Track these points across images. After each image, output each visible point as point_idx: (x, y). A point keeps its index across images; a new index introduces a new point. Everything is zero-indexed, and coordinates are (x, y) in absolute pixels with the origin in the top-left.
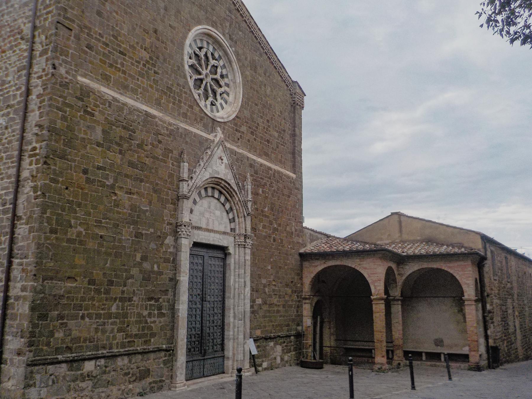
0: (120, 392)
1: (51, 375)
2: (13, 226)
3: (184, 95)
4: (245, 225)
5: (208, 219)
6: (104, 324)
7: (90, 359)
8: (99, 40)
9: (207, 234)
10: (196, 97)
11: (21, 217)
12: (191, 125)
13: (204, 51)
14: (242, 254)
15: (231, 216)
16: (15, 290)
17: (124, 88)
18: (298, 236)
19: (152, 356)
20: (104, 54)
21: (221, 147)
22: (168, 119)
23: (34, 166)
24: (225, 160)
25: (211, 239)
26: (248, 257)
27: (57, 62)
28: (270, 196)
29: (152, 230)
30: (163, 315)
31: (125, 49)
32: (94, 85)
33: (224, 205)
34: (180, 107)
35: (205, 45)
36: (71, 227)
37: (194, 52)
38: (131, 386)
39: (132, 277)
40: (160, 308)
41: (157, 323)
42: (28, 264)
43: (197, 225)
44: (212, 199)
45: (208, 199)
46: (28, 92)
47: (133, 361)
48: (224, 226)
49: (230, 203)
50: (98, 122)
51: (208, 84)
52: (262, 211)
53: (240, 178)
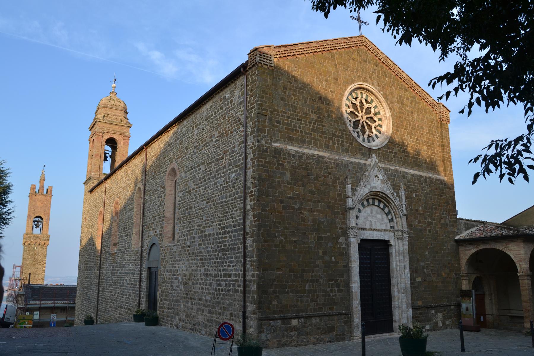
0: (315, 340)
1: (272, 326)
2: (245, 239)
3: (345, 136)
4: (402, 223)
5: (371, 222)
6: (301, 297)
7: (295, 318)
8: (284, 116)
9: (371, 232)
10: (355, 135)
11: (248, 233)
12: (353, 156)
13: (359, 99)
14: (401, 245)
15: (390, 217)
16: (249, 277)
17: (301, 142)
18: (453, 226)
19: (336, 318)
20: (288, 123)
21: (376, 168)
22: (335, 156)
23: (252, 203)
24: (381, 177)
25: (375, 236)
26: (406, 247)
27: (259, 138)
28: (423, 198)
29: (329, 234)
30: (342, 291)
31: (300, 116)
32: (283, 146)
33: (383, 210)
34: (343, 145)
35: (359, 94)
36: (276, 237)
37: (352, 102)
38: (322, 336)
39: (317, 266)
40: (338, 286)
42: (254, 261)
43: (363, 227)
44: (373, 206)
45: (370, 207)
46: (246, 157)
47: (323, 320)
48: (384, 225)
49: (388, 207)
50: (286, 169)
51: (364, 123)
52: (417, 210)
53: (396, 188)
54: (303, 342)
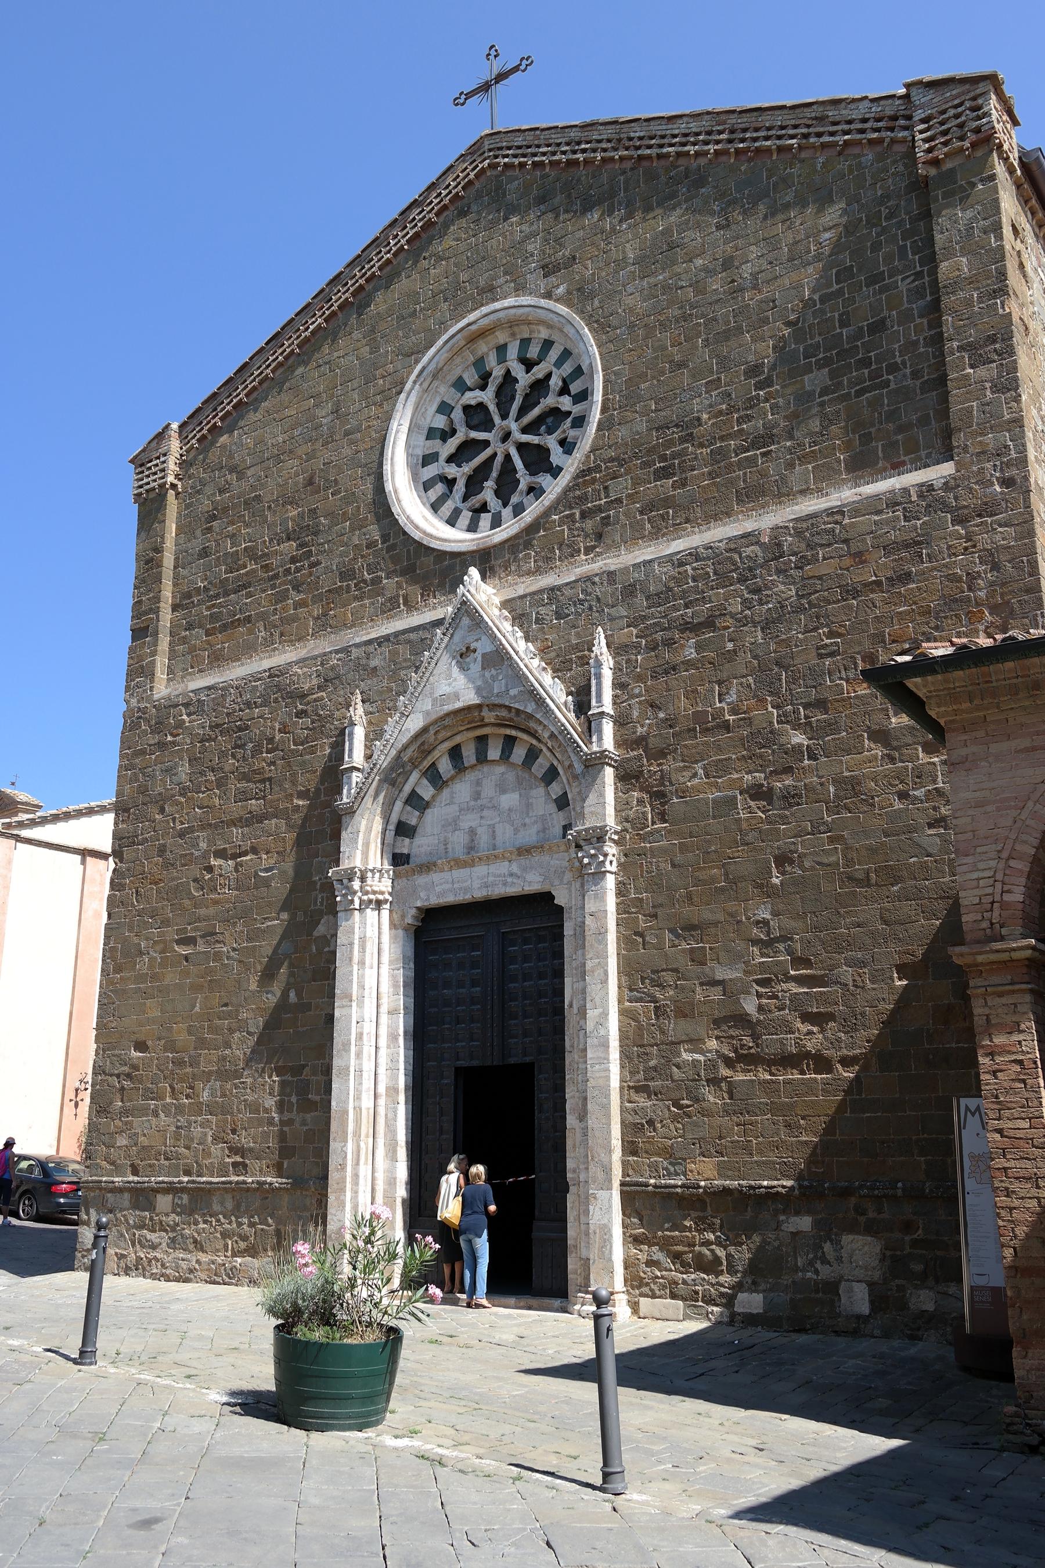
5: (472, 832)
15: (556, 790)
36: (141, 953)
41: (297, 1125)
48: (534, 830)
54: (177, 1268)
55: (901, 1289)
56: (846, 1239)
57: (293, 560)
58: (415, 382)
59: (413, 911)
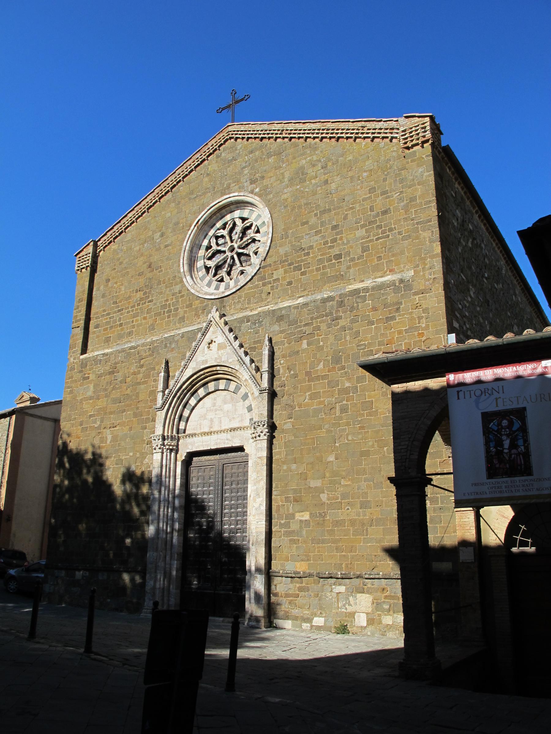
3: (180, 300)
55: (379, 615)
56: (359, 595)
57: (141, 299)
58: (195, 226)
59: (185, 454)
